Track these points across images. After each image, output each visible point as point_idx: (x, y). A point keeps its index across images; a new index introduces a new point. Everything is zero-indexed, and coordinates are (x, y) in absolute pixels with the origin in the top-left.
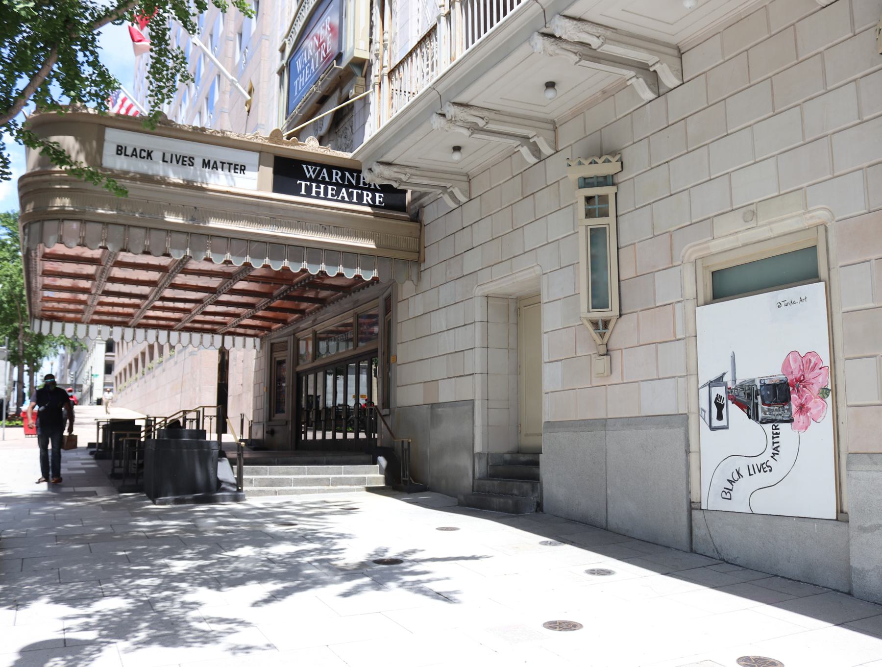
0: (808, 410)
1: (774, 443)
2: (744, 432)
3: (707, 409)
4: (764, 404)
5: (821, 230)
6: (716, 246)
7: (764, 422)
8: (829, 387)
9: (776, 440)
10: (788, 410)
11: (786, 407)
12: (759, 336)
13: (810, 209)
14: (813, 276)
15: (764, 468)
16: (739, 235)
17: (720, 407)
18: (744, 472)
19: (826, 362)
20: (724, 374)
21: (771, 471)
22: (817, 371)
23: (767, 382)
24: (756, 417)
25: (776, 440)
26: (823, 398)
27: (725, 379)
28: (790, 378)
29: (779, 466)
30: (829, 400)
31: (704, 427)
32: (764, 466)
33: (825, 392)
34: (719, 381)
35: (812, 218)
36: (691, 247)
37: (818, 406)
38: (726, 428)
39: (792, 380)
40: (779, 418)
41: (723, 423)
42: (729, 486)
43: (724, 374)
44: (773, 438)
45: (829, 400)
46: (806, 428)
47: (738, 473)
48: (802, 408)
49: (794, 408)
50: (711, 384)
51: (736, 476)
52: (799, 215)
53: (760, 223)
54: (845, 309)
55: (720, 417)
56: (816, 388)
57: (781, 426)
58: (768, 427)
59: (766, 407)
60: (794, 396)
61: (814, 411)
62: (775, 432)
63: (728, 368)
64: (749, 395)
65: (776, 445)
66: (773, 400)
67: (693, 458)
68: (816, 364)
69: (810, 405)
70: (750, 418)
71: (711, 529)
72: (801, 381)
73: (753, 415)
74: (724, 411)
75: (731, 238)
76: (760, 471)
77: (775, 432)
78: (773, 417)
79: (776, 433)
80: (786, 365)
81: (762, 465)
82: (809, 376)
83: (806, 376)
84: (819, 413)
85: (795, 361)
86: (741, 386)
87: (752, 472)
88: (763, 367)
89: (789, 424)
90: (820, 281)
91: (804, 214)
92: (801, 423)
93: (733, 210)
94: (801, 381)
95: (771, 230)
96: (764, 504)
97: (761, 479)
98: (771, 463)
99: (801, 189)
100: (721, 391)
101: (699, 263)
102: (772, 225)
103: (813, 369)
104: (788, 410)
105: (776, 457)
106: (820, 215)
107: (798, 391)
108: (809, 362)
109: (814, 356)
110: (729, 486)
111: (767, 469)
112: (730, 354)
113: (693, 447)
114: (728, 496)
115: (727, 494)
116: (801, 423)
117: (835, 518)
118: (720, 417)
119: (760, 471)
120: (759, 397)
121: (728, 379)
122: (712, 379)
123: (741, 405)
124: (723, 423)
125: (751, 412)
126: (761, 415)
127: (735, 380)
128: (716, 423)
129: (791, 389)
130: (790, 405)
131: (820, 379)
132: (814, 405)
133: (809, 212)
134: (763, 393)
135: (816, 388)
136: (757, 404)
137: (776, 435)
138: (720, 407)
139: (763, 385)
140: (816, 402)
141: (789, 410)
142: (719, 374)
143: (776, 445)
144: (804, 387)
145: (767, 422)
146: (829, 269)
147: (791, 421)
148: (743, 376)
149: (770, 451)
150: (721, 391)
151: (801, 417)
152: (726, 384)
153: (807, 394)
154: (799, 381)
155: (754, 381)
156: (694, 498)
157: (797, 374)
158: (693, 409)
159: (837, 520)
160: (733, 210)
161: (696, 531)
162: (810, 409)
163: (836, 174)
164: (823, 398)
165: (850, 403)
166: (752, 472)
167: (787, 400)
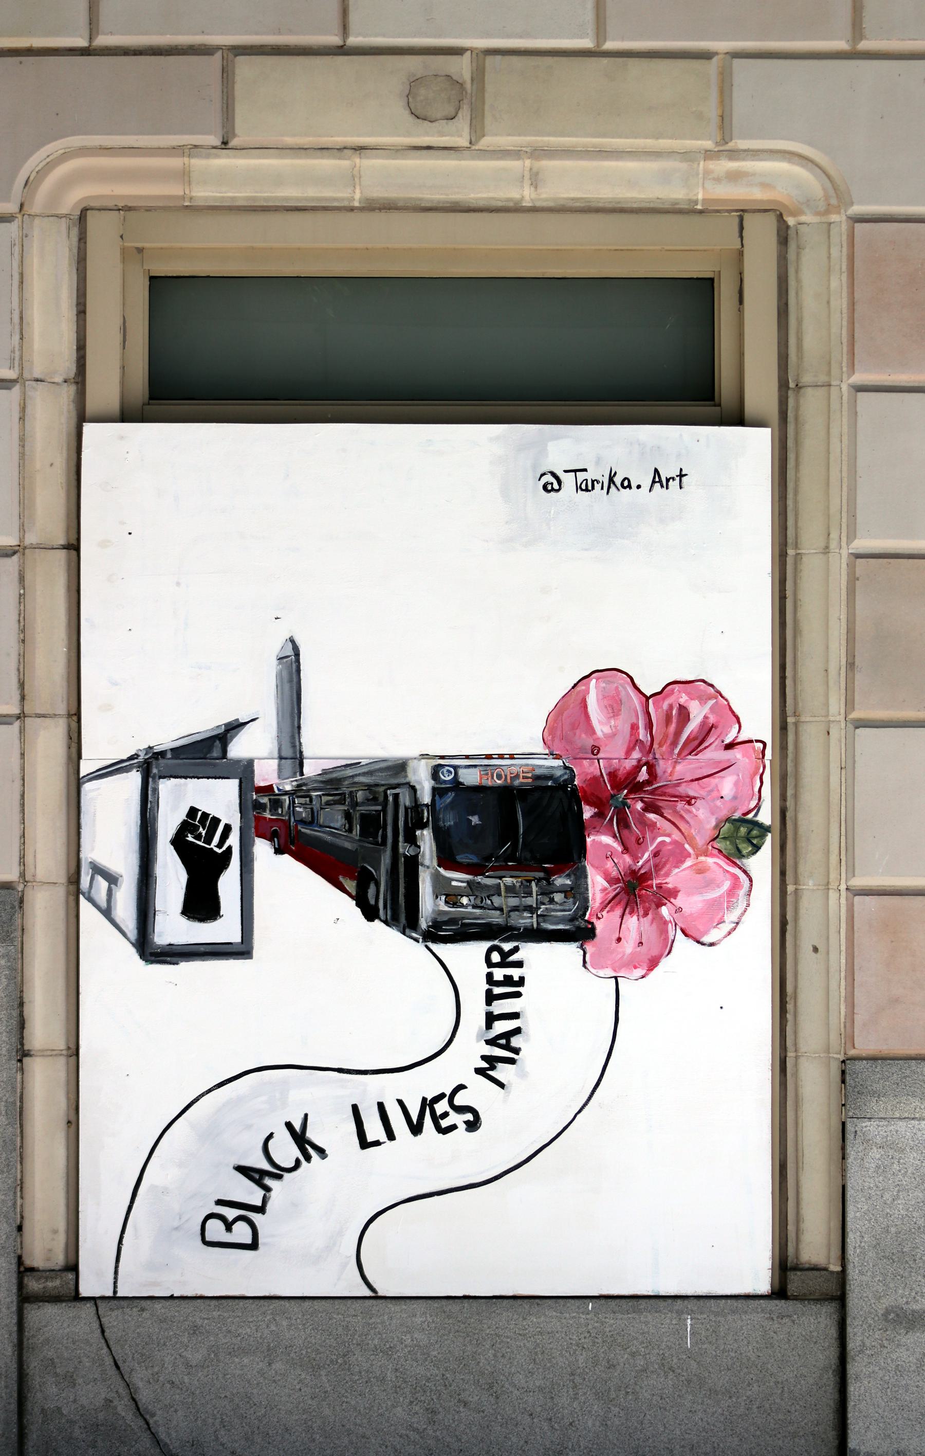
0: (666, 895)
1: (491, 1019)
2: (327, 971)
3: (126, 865)
4: (446, 859)
5: (761, 234)
6: (224, 176)
7: (438, 933)
8: (765, 817)
9: (499, 1007)
10: (567, 892)
11: (561, 881)
12: (432, 588)
13: (742, 144)
14: (693, 392)
15: (428, 1116)
16: (370, 164)
17: (204, 869)
18: (331, 1131)
19: (758, 722)
20: (235, 727)
21: (472, 1126)
22: (713, 754)
23: (470, 778)
24: (402, 914)
25: (499, 1007)
26: (735, 856)
27: (238, 749)
28: (584, 771)
29: (513, 1113)
30: (761, 864)
31: (106, 948)
32: (442, 1107)
33: (741, 835)
34: (205, 754)
35: (734, 177)
36: (84, 151)
37: (710, 884)
38: (241, 950)
39: (596, 780)
40: (525, 920)
41: (225, 929)
42: (251, 1194)
43: (235, 727)
44: (490, 998)
45: (761, 864)
46: (653, 964)
47: (300, 1138)
48: (635, 891)
49: (597, 884)
50: (152, 766)
51: (285, 1151)
52: (687, 156)
53: (486, 142)
54: (863, 544)
55: (201, 903)
56: (704, 818)
57: (529, 952)
58: (469, 959)
59: (458, 879)
60: (600, 841)
61: (690, 903)
62: (499, 974)
63: (259, 700)
64: (371, 826)
65: (501, 1027)
66: (504, 851)
67: (43, 1079)
68: (707, 730)
69: (675, 877)
70: (370, 914)
71: (139, 1378)
72: (637, 788)
73: (388, 899)
74: (228, 885)
75: (326, 164)
76: (416, 1129)
77: (499, 974)
78: (496, 918)
79: (508, 981)
80: (568, 716)
81: (428, 1104)
82: (677, 770)
83: (662, 766)
84: (714, 913)
85: (613, 706)
86: (333, 783)
87: (375, 1130)
88: (491, 720)
89: (569, 951)
90: (738, 419)
91: (708, 155)
92: (628, 946)
93: (342, 50)
94: (637, 788)
95: (535, 179)
96: (423, 1259)
97: (419, 1158)
98: (479, 1093)
99: (706, 56)
100: (220, 798)
101: (102, 229)
102: (547, 164)
103: (697, 744)
104: (567, 892)
105: (502, 1072)
106: (772, 174)
107: (623, 823)
108: (679, 719)
109: (703, 699)
110: (251, 1194)
111: (455, 1118)
112: (276, 646)
113: (44, 1029)
114: (242, 1233)
115: (235, 1224)
116: (628, 946)
117: (763, 1285)
118: (201, 903)
119: (416, 1129)
120: (426, 839)
121: (256, 746)
122: (166, 736)
123: (327, 863)
124: (225, 929)
125: (378, 894)
126: (429, 904)
127: (292, 755)
128: (172, 927)
129: (588, 812)
130: (581, 875)
131: (727, 785)
132: (692, 883)
133: (734, 154)
134: (449, 820)
135: (704, 818)
136: (413, 864)
137: (504, 986)
138: (204, 869)
139: (450, 789)
140: (701, 870)
141: (578, 892)
142: (202, 722)
143: (501, 1027)
144: (658, 811)
145: (462, 933)
146: (783, 385)
147: (580, 933)
148: (338, 738)
149: (472, 1046)
150: (220, 798)
151: (632, 922)
152: (244, 771)
153: (665, 835)
154: (628, 782)
155: (401, 767)
156: (43, 1248)
157: (617, 756)
158: (48, 861)
159: (780, 1292)
160: (342, 50)
161: (47, 1392)
162: (674, 893)
163: (864, 45)
164: (735, 856)
165: (859, 882)
166: (375, 1130)
167: (568, 853)
